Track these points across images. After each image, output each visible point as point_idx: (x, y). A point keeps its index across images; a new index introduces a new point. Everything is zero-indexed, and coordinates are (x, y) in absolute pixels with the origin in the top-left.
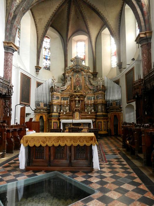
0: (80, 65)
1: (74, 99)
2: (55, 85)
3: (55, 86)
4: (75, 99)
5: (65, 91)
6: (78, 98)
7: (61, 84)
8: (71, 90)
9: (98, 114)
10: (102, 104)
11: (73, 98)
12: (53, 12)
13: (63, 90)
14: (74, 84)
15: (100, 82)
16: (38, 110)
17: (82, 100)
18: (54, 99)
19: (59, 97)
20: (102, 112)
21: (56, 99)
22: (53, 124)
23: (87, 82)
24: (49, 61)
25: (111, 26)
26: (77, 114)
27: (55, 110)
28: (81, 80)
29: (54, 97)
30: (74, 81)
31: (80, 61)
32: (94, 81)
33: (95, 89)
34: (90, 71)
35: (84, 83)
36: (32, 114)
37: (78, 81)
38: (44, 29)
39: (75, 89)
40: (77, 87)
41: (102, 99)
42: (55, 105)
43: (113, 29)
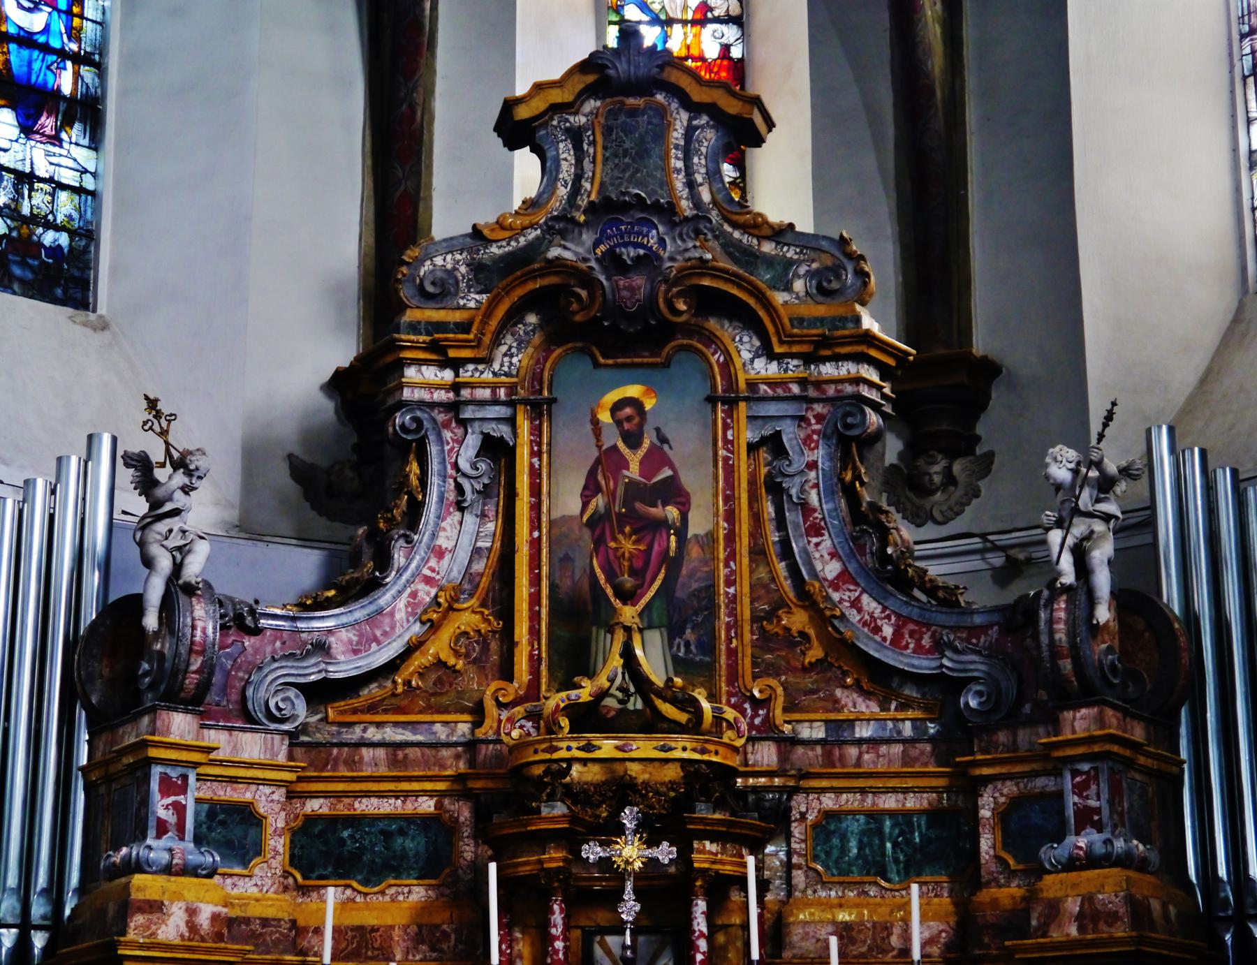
0: (685, 204)
1: (554, 857)
2: (194, 569)
4: (592, 852)
5: (372, 691)
6: (651, 833)
8: (507, 673)
11: (543, 840)
14: (562, 561)
15: (1079, 528)
18: (157, 849)
19: (247, 816)
21: (187, 851)
23: (815, 530)
24: (76, 132)
28: (688, 480)
29: (161, 808)
31: (677, 135)
32: (918, 519)
34: (869, 323)
35: (758, 553)
40: (628, 614)
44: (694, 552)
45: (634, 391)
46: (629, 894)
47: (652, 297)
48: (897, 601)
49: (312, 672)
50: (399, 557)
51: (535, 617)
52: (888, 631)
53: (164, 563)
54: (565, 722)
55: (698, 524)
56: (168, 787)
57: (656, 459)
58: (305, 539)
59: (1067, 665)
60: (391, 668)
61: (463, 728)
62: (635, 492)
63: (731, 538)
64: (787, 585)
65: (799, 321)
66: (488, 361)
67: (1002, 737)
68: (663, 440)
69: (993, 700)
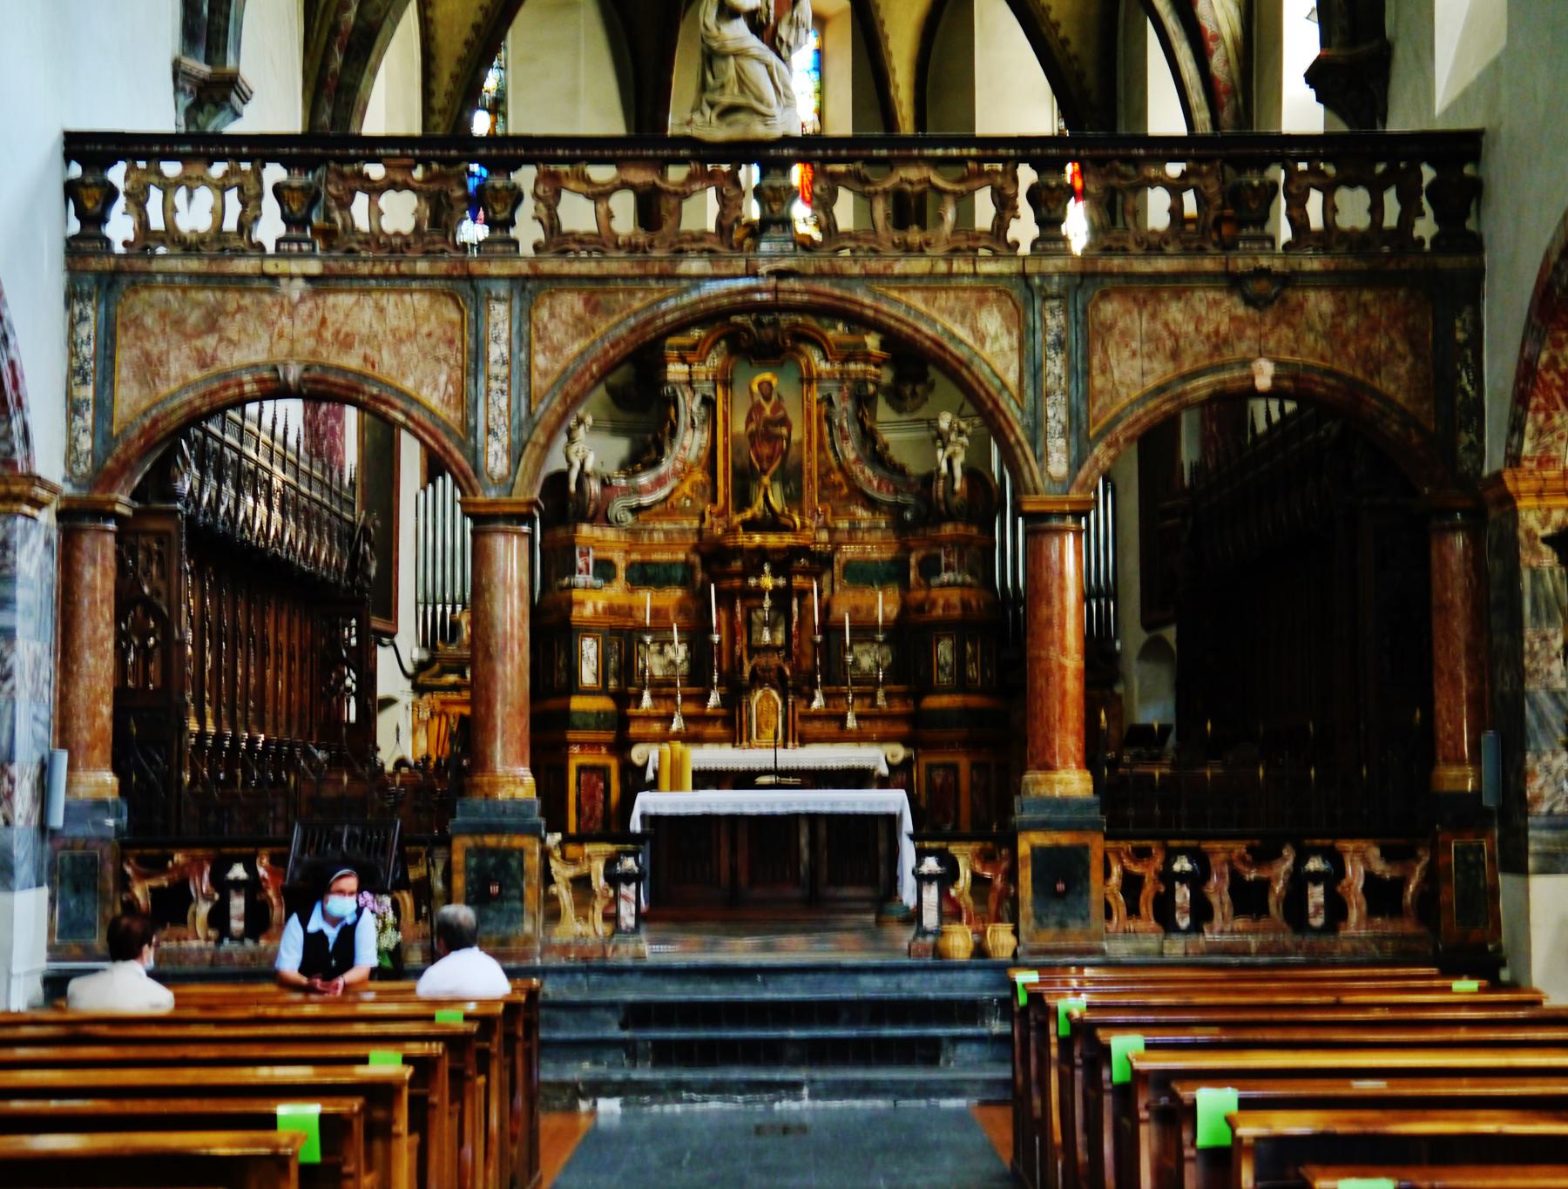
1: (737, 583)
2: (589, 467)
3: (583, 476)
4: (753, 582)
7: (620, 447)
8: (714, 500)
9: (934, 702)
10: (961, 628)
13: (649, 507)
14: (737, 452)
15: (950, 449)
16: (445, 671)
18: (580, 579)
20: (961, 685)
22: (578, 783)
23: (845, 438)
26: (764, 703)
27: (588, 675)
29: (580, 563)
30: (739, 426)
32: (899, 410)
33: (910, 500)
35: (821, 447)
37: (768, 431)
39: (743, 501)
42: (587, 630)
43: (1056, 25)
44: (793, 450)
46: (767, 596)
47: (776, 338)
48: (880, 471)
49: (634, 502)
50: (667, 451)
51: (726, 476)
52: (875, 483)
53: (577, 465)
54: (741, 529)
55: (795, 436)
56: (582, 555)
58: (616, 431)
59: (943, 507)
60: (666, 499)
61: (696, 523)
62: (769, 422)
63: (809, 442)
64: (834, 462)
65: (839, 345)
66: (704, 362)
68: (779, 397)
69: (916, 517)
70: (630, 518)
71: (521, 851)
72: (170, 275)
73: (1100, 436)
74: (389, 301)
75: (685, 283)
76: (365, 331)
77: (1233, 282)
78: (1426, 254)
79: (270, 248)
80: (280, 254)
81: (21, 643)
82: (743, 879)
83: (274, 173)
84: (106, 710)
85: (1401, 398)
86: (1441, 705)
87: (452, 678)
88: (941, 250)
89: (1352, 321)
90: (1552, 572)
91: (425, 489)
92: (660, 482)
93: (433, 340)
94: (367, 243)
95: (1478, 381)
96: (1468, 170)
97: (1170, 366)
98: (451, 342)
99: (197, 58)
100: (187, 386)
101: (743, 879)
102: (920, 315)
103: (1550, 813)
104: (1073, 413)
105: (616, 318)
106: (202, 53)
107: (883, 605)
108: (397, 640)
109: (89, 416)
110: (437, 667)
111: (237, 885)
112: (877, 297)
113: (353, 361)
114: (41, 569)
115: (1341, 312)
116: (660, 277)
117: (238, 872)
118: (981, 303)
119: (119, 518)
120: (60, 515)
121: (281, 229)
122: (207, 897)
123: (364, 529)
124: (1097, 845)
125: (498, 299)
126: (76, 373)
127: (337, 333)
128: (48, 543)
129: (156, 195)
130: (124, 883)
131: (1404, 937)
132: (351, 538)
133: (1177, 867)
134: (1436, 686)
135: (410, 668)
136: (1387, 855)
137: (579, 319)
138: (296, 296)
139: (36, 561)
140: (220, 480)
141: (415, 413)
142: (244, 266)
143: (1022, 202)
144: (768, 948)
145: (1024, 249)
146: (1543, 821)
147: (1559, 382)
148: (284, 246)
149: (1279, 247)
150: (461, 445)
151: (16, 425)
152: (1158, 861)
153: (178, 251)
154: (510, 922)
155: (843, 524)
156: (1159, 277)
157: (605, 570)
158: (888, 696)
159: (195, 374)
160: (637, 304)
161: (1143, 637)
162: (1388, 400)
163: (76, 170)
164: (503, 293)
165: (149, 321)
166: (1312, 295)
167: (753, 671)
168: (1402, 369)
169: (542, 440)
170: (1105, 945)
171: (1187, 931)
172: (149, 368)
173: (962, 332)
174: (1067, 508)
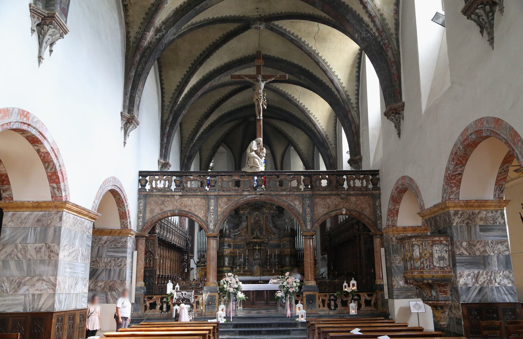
4: (255, 248)
7: (232, 225)
8: (248, 234)
12: (226, 132)
16: (202, 263)
17: (263, 250)
18: (225, 247)
25: (302, 151)
27: (226, 264)
28: (261, 220)
29: (225, 245)
30: (252, 221)
36: (195, 269)
38: (212, 150)
39: (253, 233)
41: (290, 248)
42: (226, 256)
43: (304, 155)
45: (257, 213)
55: (262, 223)
56: (226, 243)
57: (258, 218)
67: (283, 239)
70: (233, 237)
71: (215, 296)
72: (156, 195)
73: (316, 222)
74: (193, 199)
75: (244, 196)
76: (189, 204)
77: (338, 195)
78: (371, 190)
79: (173, 191)
80: (175, 191)
81: (128, 259)
82: (255, 300)
83: (174, 178)
84: (143, 271)
85: (368, 215)
86: (376, 269)
87: (203, 264)
88: (288, 190)
89: (359, 202)
90: (395, 245)
91: (199, 232)
92: (239, 231)
93: (201, 206)
94: (190, 189)
95: (381, 212)
96: (377, 176)
97: (328, 210)
98: (204, 206)
99: (162, 159)
100: (158, 214)
101: (255, 300)
102: (285, 201)
103: (397, 288)
104: (312, 218)
105: (232, 202)
106: (163, 158)
107: (277, 252)
108: (194, 258)
109: (141, 219)
110: (201, 262)
111: (165, 302)
112: (277, 198)
113: (187, 210)
114: (132, 246)
115: (357, 201)
116: (240, 195)
117: (165, 300)
118: (295, 199)
119: (146, 237)
120: (136, 237)
121: (175, 187)
122: (159, 304)
123: (189, 239)
124: (317, 294)
125: (212, 199)
126: (139, 212)
127: (184, 205)
128: (133, 241)
129: (154, 182)
130: (145, 302)
131: (372, 310)
132: (186, 241)
133: (331, 298)
134: (376, 265)
135: (196, 263)
136: (369, 295)
137: (226, 202)
138: (177, 198)
139: (131, 244)
140: (164, 230)
141: (198, 219)
142: (169, 193)
143: (302, 182)
144: (259, 313)
145: (302, 190)
146: (396, 289)
147: (395, 212)
148: (176, 190)
149: (346, 190)
150: (205, 224)
151: (128, 221)
152: (328, 297)
153: (157, 191)
154: (213, 309)
155: (270, 238)
156: (326, 195)
157: (229, 246)
158: (278, 267)
159: (160, 212)
160: (236, 200)
161: (321, 257)
162: (365, 216)
163: (141, 177)
164: (213, 198)
165: (152, 203)
166: (352, 197)
167: (255, 263)
168: (368, 210)
169: (220, 223)
170: (319, 312)
171: (333, 310)
172: (152, 211)
173: (292, 204)
174: (311, 234)
